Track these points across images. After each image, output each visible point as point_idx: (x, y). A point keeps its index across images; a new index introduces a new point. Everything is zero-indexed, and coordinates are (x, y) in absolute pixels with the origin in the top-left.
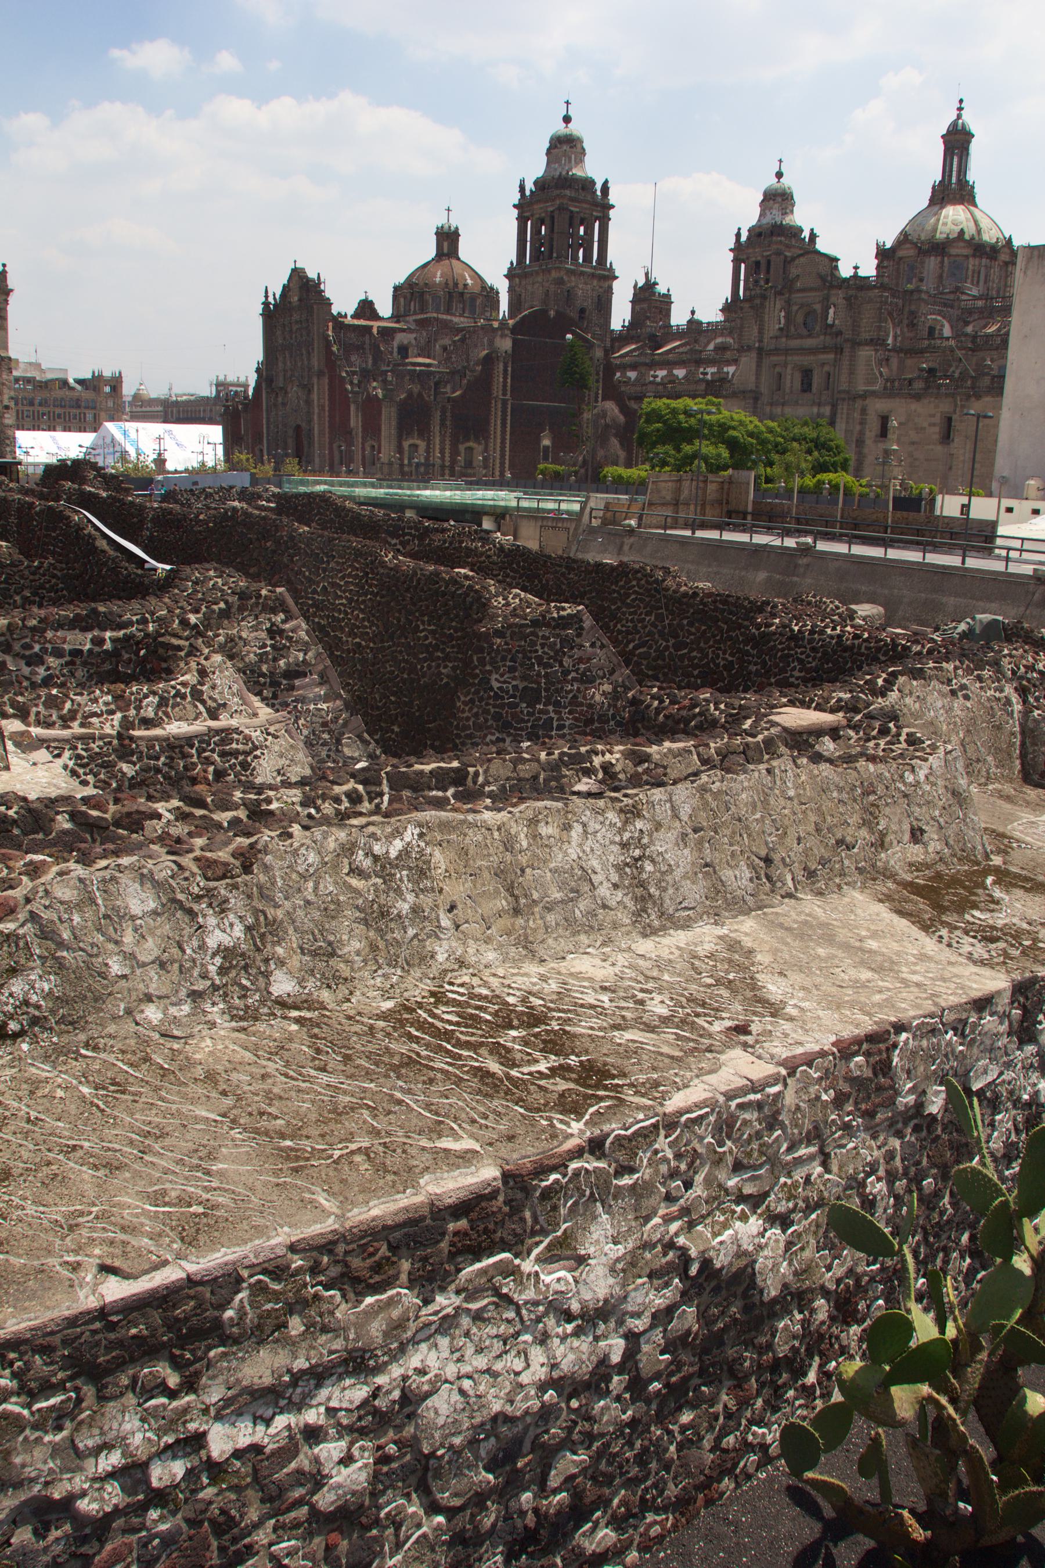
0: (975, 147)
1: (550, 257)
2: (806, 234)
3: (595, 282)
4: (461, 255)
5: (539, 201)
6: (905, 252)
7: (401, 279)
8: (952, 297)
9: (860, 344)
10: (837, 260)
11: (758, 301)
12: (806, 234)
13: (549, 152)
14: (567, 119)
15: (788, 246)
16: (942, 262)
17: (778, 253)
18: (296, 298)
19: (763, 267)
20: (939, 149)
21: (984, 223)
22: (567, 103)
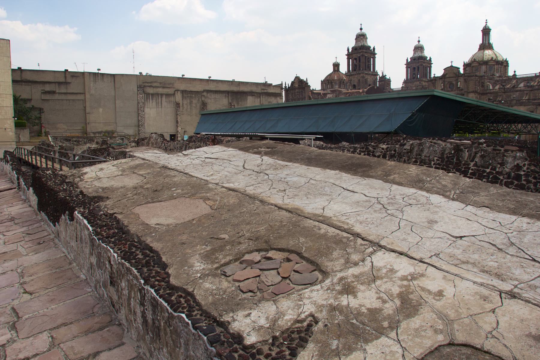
0: (492, 33)
1: (360, 70)
2: (428, 59)
3: (373, 77)
4: (340, 70)
5: (354, 54)
6: (475, 64)
7: (323, 78)
8: (491, 77)
9: (469, 93)
10: (459, 68)
11: (434, 81)
12: (428, 59)
13: (356, 39)
14: (361, 29)
15: (424, 63)
16: (487, 67)
17: (422, 65)
18: (297, 85)
19: (416, 69)
20: (481, 34)
21: (498, 55)
22: (361, 24)
